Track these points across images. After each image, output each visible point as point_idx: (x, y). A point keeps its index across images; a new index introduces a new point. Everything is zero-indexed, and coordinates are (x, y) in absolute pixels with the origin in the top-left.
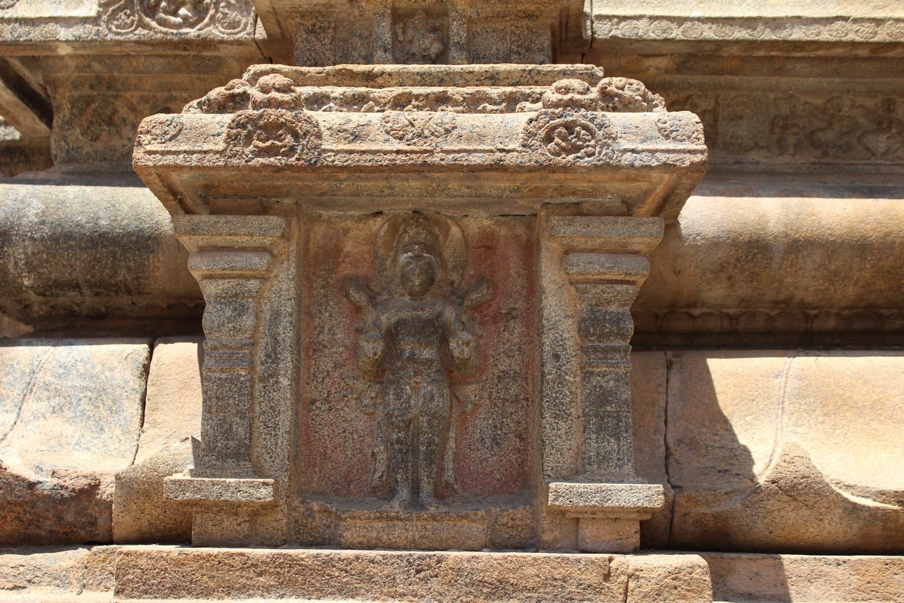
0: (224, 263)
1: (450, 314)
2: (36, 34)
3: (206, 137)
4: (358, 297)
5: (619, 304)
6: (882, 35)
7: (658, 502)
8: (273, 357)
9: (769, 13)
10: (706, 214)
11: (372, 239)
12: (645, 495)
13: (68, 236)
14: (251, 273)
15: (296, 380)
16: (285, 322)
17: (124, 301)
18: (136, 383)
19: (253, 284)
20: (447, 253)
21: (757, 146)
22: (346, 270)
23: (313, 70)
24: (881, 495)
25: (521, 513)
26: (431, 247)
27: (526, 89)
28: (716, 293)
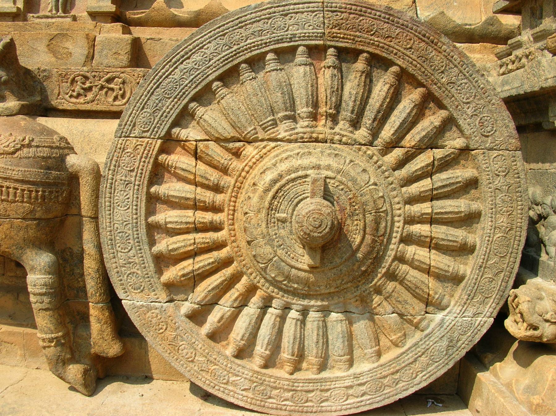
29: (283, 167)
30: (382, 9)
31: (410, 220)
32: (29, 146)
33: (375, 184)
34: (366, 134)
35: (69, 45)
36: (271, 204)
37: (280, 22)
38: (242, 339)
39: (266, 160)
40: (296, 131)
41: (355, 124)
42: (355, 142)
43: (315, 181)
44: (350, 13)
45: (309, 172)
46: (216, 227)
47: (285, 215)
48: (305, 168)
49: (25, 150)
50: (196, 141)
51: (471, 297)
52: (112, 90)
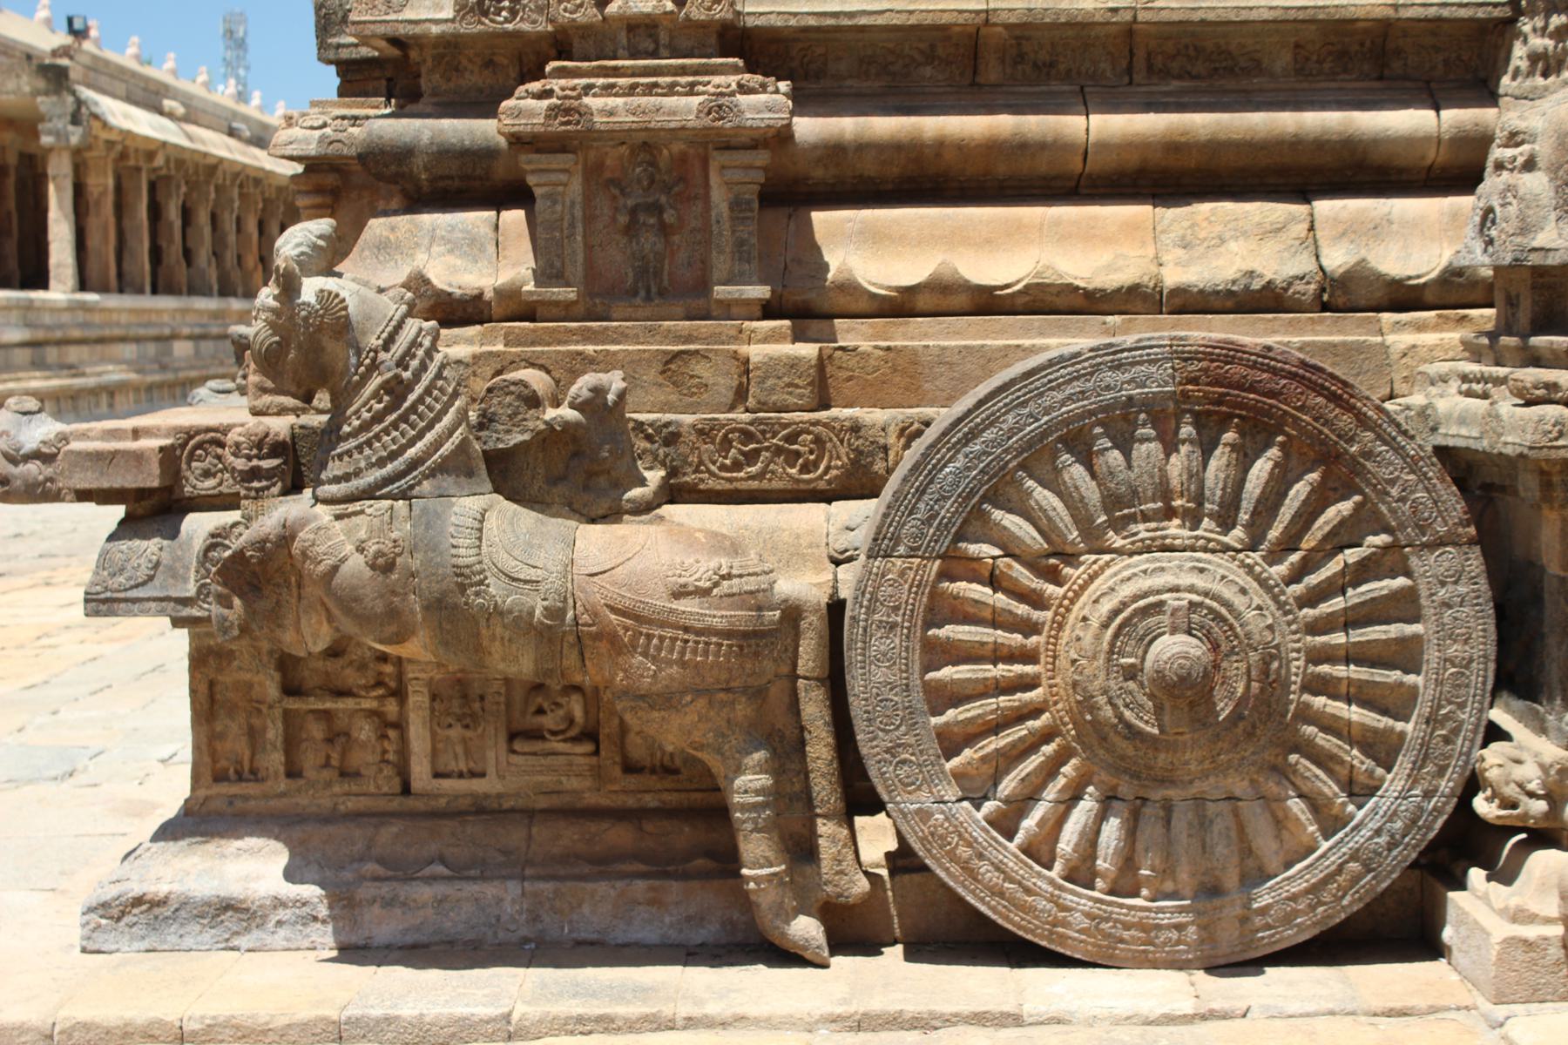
1: (663, 199)
2: (418, 30)
3: (531, 114)
4: (616, 192)
5: (751, 193)
6: (913, 20)
7: (768, 295)
8: (572, 225)
9: (847, 8)
10: (808, 128)
11: (621, 157)
12: (761, 292)
13: (447, 151)
14: (559, 182)
15: (584, 236)
16: (578, 207)
17: (477, 184)
18: (491, 234)
19: (560, 189)
20: (661, 165)
21: (851, 77)
22: (607, 175)
23: (586, 64)
24: (889, 288)
25: (702, 302)
26: (653, 164)
28: (819, 173)
29: (1127, 591)
30: (1258, 349)
31: (1317, 656)
32: (729, 576)
33: (1259, 608)
35: (700, 369)
36: (1112, 644)
37: (1109, 377)
38: (1074, 851)
39: (1097, 582)
40: (1140, 536)
41: (1226, 524)
42: (1226, 548)
43: (1175, 611)
44: (1212, 361)
46: (1029, 684)
47: (1132, 660)
48: (1158, 592)
50: (994, 558)
51: (1418, 766)
52: (798, 454)
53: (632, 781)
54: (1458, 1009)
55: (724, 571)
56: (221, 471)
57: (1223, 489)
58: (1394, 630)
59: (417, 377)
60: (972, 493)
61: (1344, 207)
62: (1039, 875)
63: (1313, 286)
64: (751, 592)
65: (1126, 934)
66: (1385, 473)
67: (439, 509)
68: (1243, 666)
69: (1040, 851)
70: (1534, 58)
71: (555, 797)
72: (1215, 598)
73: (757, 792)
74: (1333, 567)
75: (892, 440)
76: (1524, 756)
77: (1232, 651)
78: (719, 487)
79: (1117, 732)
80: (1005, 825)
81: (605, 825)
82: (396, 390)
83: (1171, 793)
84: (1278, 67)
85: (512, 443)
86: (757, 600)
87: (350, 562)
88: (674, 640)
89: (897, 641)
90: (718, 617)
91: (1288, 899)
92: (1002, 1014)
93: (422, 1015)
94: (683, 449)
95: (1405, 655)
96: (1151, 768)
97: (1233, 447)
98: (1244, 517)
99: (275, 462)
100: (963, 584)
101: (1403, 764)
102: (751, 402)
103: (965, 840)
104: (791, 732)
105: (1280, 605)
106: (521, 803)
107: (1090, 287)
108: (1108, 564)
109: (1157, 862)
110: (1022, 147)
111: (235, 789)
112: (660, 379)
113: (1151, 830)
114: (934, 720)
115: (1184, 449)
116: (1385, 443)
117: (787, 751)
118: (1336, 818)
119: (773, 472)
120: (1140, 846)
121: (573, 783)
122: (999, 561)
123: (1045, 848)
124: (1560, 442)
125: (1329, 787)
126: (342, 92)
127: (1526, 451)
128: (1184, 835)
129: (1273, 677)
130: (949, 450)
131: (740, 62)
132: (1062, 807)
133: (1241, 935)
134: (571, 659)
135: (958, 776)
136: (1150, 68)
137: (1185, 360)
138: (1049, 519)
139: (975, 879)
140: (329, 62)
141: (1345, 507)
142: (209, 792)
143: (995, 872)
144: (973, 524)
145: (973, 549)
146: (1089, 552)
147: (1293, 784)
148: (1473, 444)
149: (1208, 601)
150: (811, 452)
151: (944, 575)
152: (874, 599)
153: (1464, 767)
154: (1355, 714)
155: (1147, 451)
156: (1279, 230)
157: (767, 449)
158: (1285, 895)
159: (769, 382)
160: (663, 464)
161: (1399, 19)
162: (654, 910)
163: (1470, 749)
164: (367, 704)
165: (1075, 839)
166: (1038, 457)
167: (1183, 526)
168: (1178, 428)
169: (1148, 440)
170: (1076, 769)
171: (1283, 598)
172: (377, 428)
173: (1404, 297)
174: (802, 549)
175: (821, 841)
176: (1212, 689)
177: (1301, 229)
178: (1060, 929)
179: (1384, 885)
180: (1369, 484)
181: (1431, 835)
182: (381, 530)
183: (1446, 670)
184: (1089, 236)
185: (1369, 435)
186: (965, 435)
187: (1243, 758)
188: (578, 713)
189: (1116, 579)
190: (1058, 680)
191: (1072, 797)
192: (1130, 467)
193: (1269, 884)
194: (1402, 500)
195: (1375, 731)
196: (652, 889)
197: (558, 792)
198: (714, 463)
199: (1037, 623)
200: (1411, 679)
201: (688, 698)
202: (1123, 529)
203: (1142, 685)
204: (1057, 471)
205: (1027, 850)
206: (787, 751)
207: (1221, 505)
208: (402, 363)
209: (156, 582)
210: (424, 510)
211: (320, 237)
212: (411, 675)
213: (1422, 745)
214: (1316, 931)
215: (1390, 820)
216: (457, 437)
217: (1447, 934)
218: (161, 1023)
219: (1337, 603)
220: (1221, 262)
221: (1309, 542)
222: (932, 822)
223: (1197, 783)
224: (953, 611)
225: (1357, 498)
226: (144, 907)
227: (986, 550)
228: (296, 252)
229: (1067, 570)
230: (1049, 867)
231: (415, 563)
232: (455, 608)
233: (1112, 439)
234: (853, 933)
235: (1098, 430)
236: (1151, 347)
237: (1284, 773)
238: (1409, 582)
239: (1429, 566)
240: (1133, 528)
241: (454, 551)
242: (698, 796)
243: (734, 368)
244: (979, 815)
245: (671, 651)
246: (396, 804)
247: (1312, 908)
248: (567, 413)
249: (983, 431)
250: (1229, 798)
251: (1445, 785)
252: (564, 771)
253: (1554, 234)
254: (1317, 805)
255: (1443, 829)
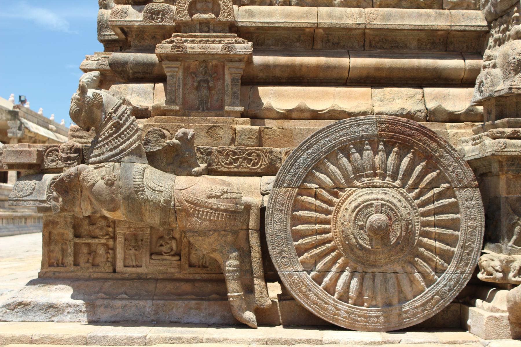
0: (170, 70)
1: (209, 78)
2: (131, 24)
3: (167, 48)
4: (193, 75)
5: (238, 77)
6: (293, 25)
8: (179, 86)
9: (272, 21)
10: (257, 59)
11: (196, 65)
12: (241, 109)
13: (139, 63)
15: (183, 90)
16: (181, 80)
17: (148, 75)
18: (152, 91)
19: (175, 73)
20: (209, 68)
21: (272, 45)
22: (191, 70)
23: (185, 34)
24: (283, 110)
25: (221, 112)
26: (206, 67)
27: (223, 39)
28: (261, 75)
29: (360, 200)
32: (227, 192)
33: (405, 207)
34: (399, 183)
35: (220, 132)
36: (355, 218)
37: (355, 129)
38: (342, 289)
39: (351, 197)
41: (394, 178)
42: (394, 187)
44: (390, 124)
45: (373, 202)
46: (327, 231)
47: (362, 223)
48: (371, 200)
49: (225, 194)
50: (316, 188)
51: (459, 262)
52: (251, 160)
53: (192, 270)
54: (473, 342)
55: (225, 190)
56: (57, 160)
57: (393, 167)
58: (451, 216)
59: (124, 123)
60: (309, 166)
61: (434, 90)
62: (330, 297)
63: (424, 114)
64: (234, 198)
65: (359, 319)
66: (447, 163)
67: (130, 166)
68: (399, 226)
69: (330, 290)
70: (495, 41)
71: (165, 274)
72: (390, 202)
73: (234, 266)
74: (430, 194)
75: (283, 156)
76: (495, 259)
77: (396, 221)
78: (224, 170)
79: (356, 248)
80: (318, 280)
81: (182, 283)
82: (117, 126)
83: (375, 270)
84: (412, 46)
85: (155, 150)
86: (236, 201)
87: (99, 182)
88: (207, 212)
89: (283, 216)
90: (223, 205)
91: (415, 308)
92: (316, 340)
93: (115, 335)
94: (213, 157)
95: (454, 225)
96: (368, 261)
97: (397, 153)
98: (400, 176)
99: (76, 155)
100: (306, 197)
101: (454, 262)
102: (236, 143)
103: (304, 284)
104: (246, 249)
105: (412, 207)
106: (153, 276)
107: (350, 112)
108: (354, 191)
109: (370, 294)
110: (328, 68)
111: (56, 269)
112: (206, 135)
113: (368, 282)
114: (295, 243)
115: (380, 153)
116: (447, 153)
117: (245, 255)
118: (431, 280)
119: (243, 166)
120: (364, 288)
121: (172, 270)
122: (318, 190)
123: (332, 289)
124: (505, 150)
125: (429, 269)
126: (104, 51)
127: (494, 152)
128: (379, 284)
129: (409, 230)
130: (302, 152)
131: (236, 35)
132: (338, 274)
133: (399, 320)
134: (172, 219)
135: (303, 263)
136: (370, 45)
137: (381, 124)
138: (335, 175)
139: (308, 299)
140: (102, 41)
141: (434, 174)
142: (47, 270)
143: (314, 297)
144: (309, 176)
145: (309, 185)
146: (348, 187)
147: (416, 268)
148: (477, 157)
149: (388, 204)
150: (256, 159)
151: (299, 194)
152: (275, 201)
153: (474, 264)
154: (438, 244)
155: (368, 153)
156: (412, 97)
157: (241, 158)
158: (414, 307)
159: (243, 137)
160: (206, 162)
161: (452, 30)
162: (198, 311)
163: (476, 257)
164: (103, 241)
165: (342, 285)
166: (331, 154)
167: (380, 179)
168: (378, 146)
169: (368, 150)
170: (343, 261)
171: (413, 204)
172: (110, 139)
173: (454, 118)
174: (252, 189)
175: (255, 286)
176: (389, 233)
177: (420, 96)
178: (336, 317)
179: (447, 304)
180: (442, 166)
181: (463, 287)
182: (110, 172)
183: (468, 230)
184: (349, 97)
185: (442, 150)
186: (307, 147)
187: (399, 258)
188: (174, 247)
189: (357, 196)
190: (337, 230)
191: (341, 271)
192: (362, 159)
193: (408, 303)
194: (453, 172)
195: (444, 250)
196: (197, 304)
197: (167, 273)
198: (223, 162)
199: (330, 211)
200: (456, 233)
201: (212, 233)
202: (360, 179)
203: (365, 232)
204: (338, 160)
205: (326, 289)
206: (245, 255)
207: (392, 172)
208: (120, 118)
209: (33, 195)
210: (125, 166)
211: (94, 76)
212: (118, 232)
213: (460, 256)
214: (424, 320)
215: (449, 281)
216: (137, 144)
217: (469, 322)
218: (25, 336)
219: (431, 206)
220: (393, 106)
221: (422, 185)
222: (293, 278)
223: (384, 267)
224: (302, 206)
225: (438, 171)
226: (22, 306)
227: (314, 186)
228: (86, 80)
229: (341, 193)
230: (333, 296)
231: (121, 184)
232: (134, 200)
233: (356, 150)
234: (265, 319)
235: (352, 146)
236: (370, 119)
237: (413, 264)
238: (455, 200)
239: (462, 194)
240: (363, 179)
241: (134, 180)
242: (214, 275)
243: (231, 132)
244: (310, 276)
245: (206, 216)
246: (110, 276)
247: (423, 311)
248: (175, 141)
249: (313, 145)
250: (395, 273)
251: (468, 270)
252: (168, 265)
253: (503, 86)
254: (424, 276)
255: (467, 285)
